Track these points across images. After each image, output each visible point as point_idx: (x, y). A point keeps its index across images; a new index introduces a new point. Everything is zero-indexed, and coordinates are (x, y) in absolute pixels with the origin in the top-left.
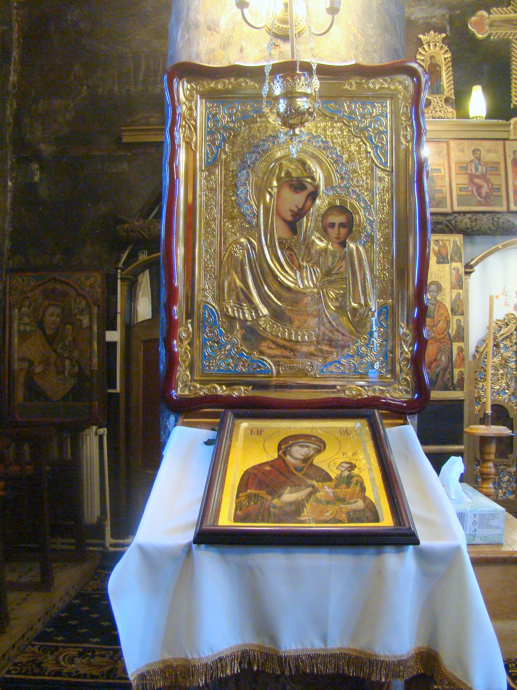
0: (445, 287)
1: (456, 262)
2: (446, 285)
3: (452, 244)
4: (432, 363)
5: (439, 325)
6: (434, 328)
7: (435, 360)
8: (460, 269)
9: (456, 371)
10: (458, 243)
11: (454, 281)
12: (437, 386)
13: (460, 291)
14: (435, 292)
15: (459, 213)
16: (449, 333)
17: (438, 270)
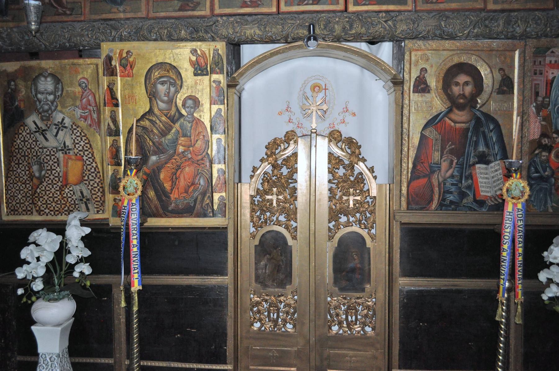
0: (203, 102)
1: (217, 73)
2: (205, 101)
3: (212, 52)
4: (189, 187)
5: (196, 145)
6: (191, 148)
7: (193, 184)
8: (222, 81)
9: (216, 196)
10: (220, 52)
11: (214, 95)
12: (195, 212)
13: (222, 107)
14: (192, 108)
15: (221, 15)
16: (207, 153)
17: (196, 83)
